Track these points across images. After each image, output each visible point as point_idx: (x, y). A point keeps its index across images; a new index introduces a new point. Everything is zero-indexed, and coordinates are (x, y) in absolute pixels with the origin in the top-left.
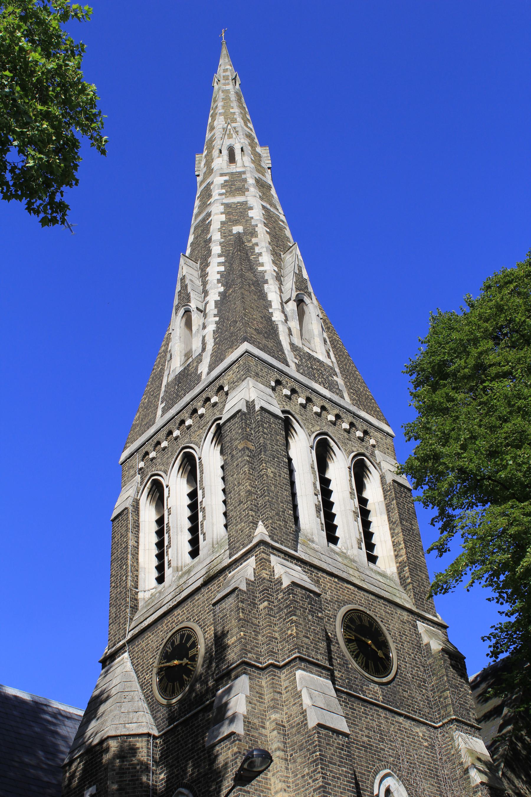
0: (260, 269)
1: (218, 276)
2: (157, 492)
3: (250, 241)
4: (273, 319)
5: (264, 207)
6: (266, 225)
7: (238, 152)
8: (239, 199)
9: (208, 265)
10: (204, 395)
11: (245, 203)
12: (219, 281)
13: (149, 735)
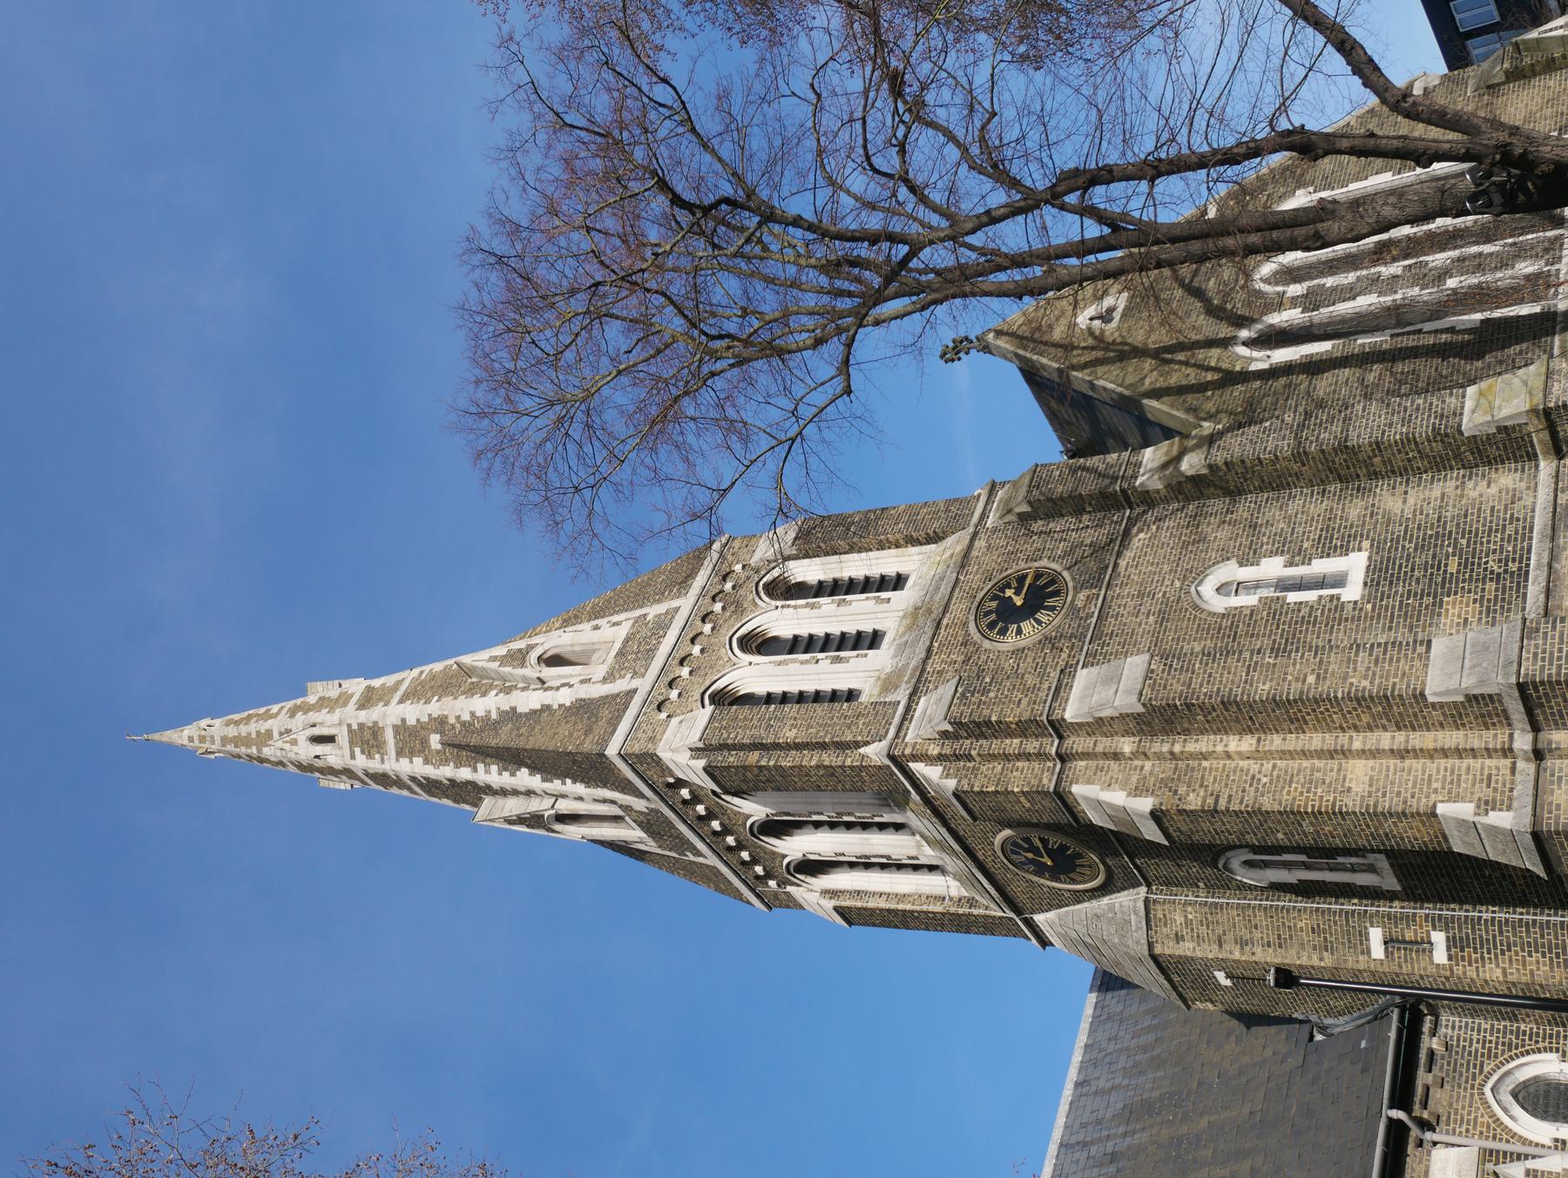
0: (494, 716)
1: (506, 774)
2: (813, 867)
3: (453, 727)
4: (568, 704)
5: (401, 702)
7: (317, 731)
8: (389, 736)
11: (396, 729)
12: (513, 774)
13: (1147, 901)
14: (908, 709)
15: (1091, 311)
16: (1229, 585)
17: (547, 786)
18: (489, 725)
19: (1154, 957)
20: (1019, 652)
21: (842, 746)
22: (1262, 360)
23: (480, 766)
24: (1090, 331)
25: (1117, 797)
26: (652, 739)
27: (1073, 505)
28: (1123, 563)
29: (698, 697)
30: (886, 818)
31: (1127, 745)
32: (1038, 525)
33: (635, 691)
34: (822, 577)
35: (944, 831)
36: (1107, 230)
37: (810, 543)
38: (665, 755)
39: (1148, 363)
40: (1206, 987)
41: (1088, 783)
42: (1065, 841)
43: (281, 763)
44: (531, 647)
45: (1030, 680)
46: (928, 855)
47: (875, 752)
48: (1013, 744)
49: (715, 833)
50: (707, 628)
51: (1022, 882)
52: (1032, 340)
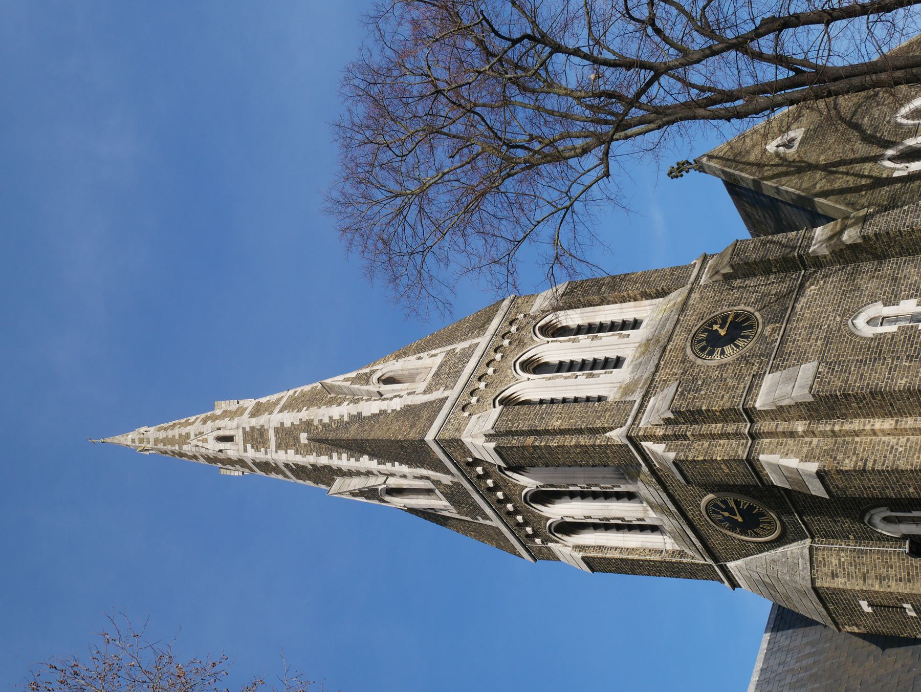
0: (346, 419)
1: (352, 460)
2: (569, 528)
3: (317, 427)
4: (398, 409)
5: (281, 411)
6: (299, 411)
7: (221, 433)
8: (272, 435)
9: (340, 470)
11: (277, 430)
12: (357, 460)
13: (811, 548)
14: (642, 406)
15: (778, 141)
16: (873, 320)
17: (381, 467)
18: (341, 424)
19: (815, 589)
20: (723, 367)
21: (594, 431)
22: (901, 170)
23: (335, 455)
24: (777, 154)
25: (792, 462)
26: (458, 430)
27: (763, 267)
28: (798, 306)
29: (491, 402)
30: (623, 488)
31: (800, 426)
32: (737, 283)
33: (447, 398)
34: (580, 323)
35: (664, 496)
36: (792, 74)
37: (575, 298)
38: (466, 440)
39: (819, 175)
40: (854, 612)
41: (771, 453)
42: (753, 503)
43: (195, 457)
44: (373, 372)
45: (730, 382)
46: (652, 517)
47: (617, 435)
48: (717, 428)
49: (499, 501)
50: (498, 356)
51: (720, 535)
52: (734, 161)
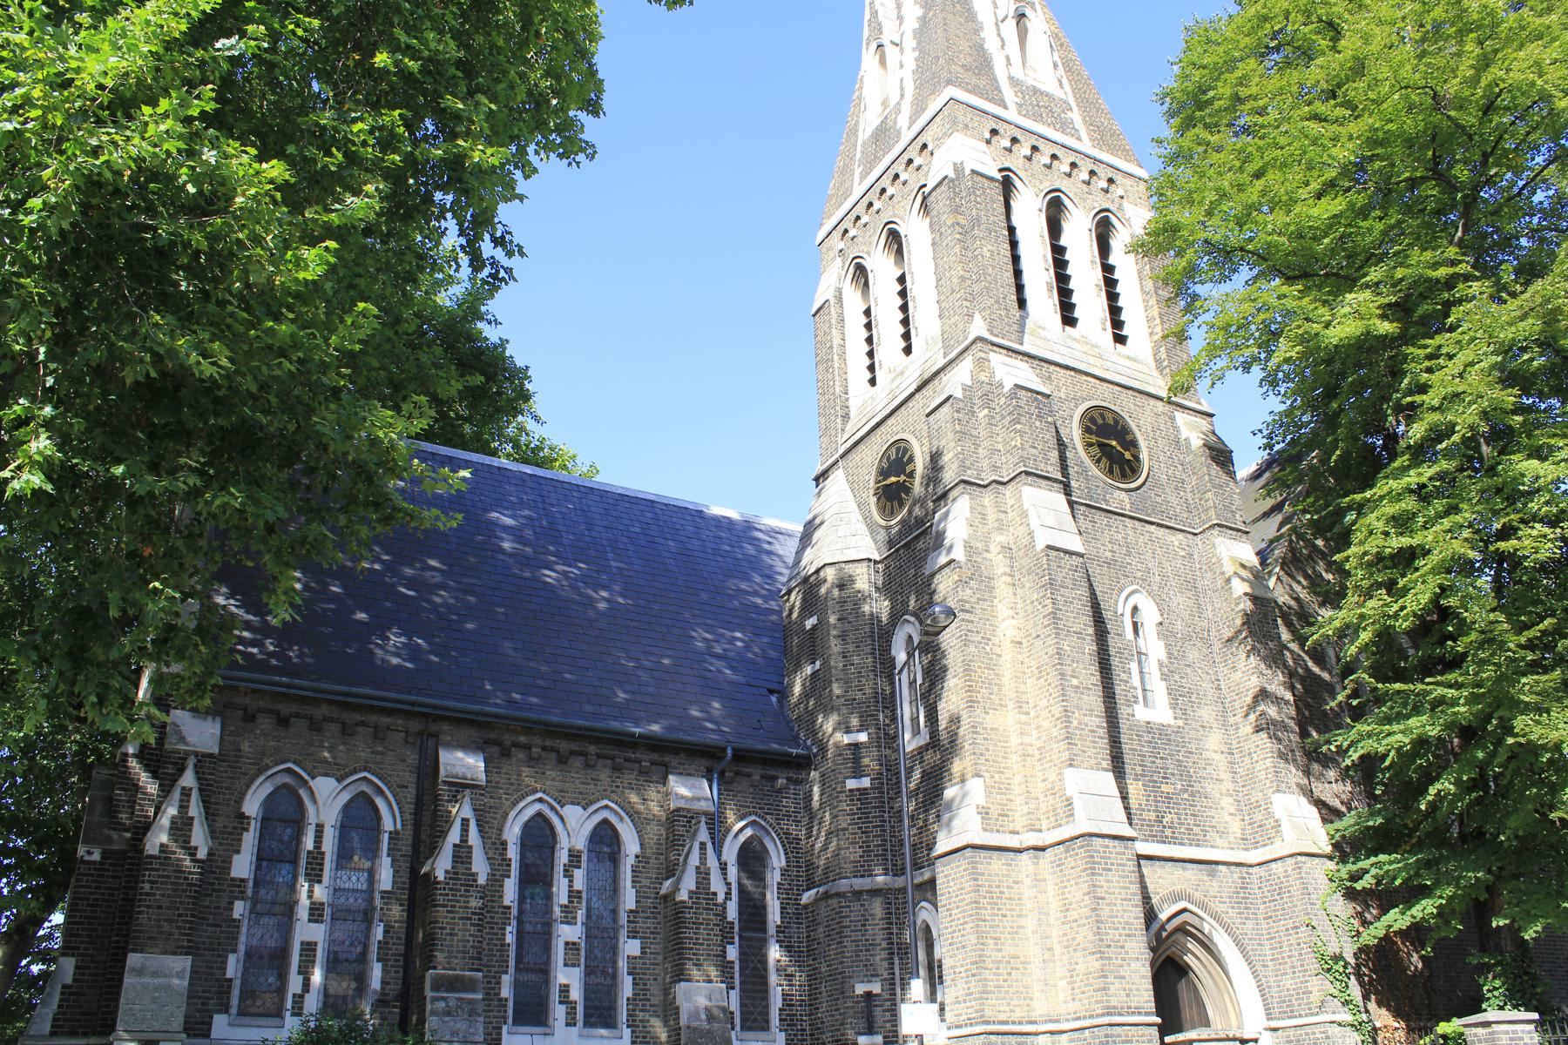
10: (906, 157)
29: (1007, 165)
33: (1006, 107)
51: (870, 456)
